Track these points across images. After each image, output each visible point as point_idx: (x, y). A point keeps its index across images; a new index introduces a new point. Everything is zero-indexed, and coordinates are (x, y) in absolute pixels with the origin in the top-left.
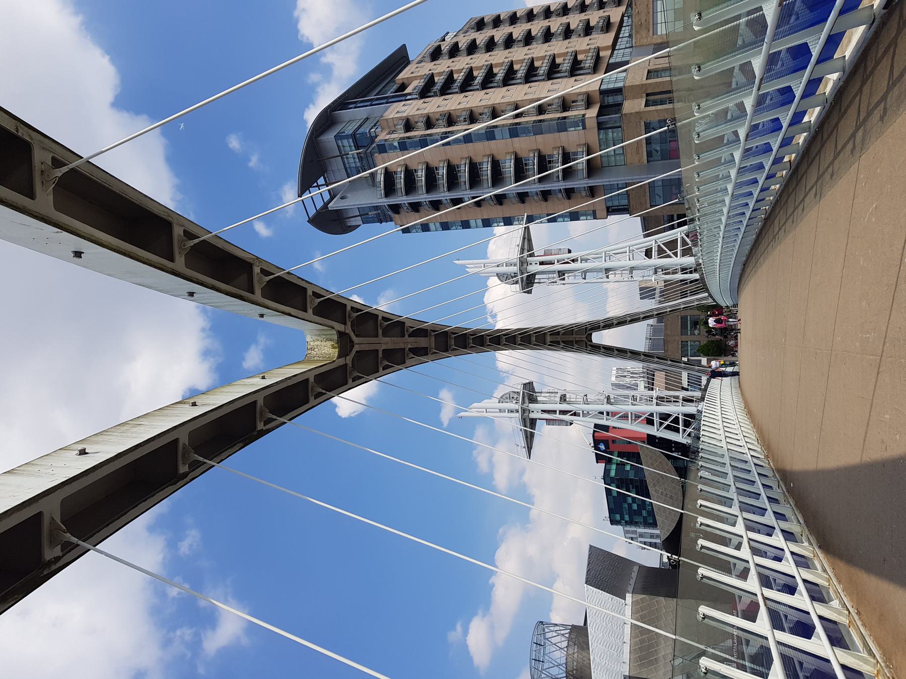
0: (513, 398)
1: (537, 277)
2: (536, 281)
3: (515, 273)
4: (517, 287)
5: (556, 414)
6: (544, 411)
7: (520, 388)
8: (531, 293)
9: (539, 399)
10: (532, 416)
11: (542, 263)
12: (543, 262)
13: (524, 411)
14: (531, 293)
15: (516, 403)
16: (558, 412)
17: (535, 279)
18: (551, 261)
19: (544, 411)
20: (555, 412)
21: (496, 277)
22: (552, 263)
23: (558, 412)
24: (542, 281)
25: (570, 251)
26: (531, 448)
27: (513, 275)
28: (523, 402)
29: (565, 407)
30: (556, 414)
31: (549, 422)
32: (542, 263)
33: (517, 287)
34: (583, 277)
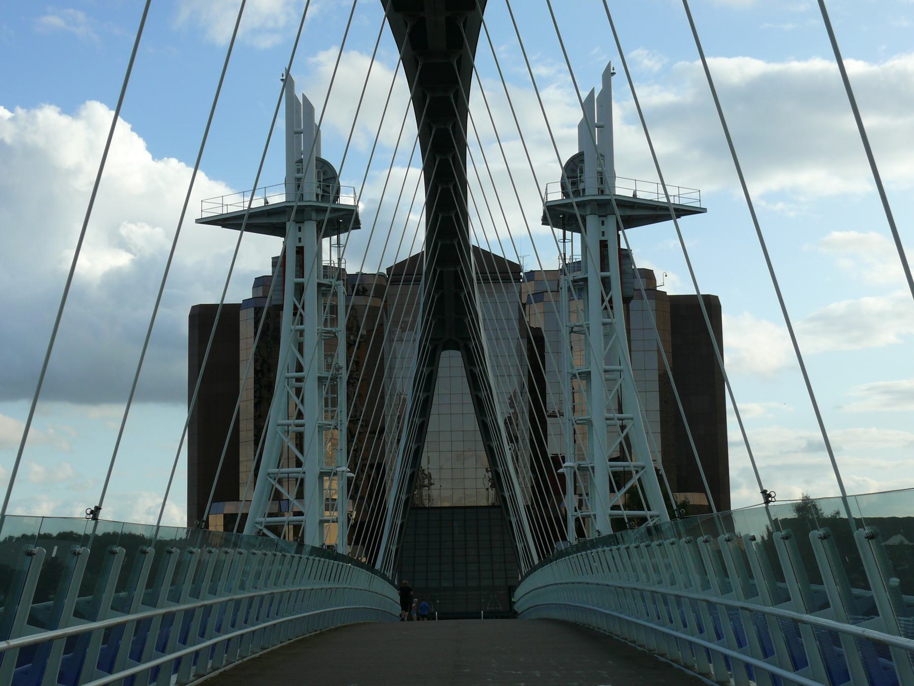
0: (328, 186)
1: (577, 236)
2: (568, 233)
3: (584, 190)
4: (556, 195)
5: (297, 277)
6: (300, 251)
7: (346, 199)
8: (543, 224)
9: (326, 242)
10: (291, 227)
11: (604, 245)
12: (606, 246)
13: (301, 210)
14: (543, 224)
15: (317, 195)
16: (300, 280)
17: (573, 231)
18: (608, 265)
19: (300, 251)
21: (575, 151)
22: (604, 266)
23: (300, 280)
24: (568, 245)
26: (224, 226)
27: (581, 186)
29: (311, 294)
30: (297, 277)
31: (279, 263)
32: (604, 245)
33: (556, 195)
34: (575, 329)
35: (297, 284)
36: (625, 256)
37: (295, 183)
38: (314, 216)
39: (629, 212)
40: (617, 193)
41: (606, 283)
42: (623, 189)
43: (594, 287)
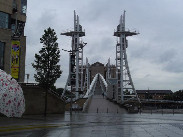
6: (76, 39)
10: (75, 35)
11: (123, 39)
13: (76, 32)
19: (76, 39)
20: (76, 42)
22: (123, 42)
25: (127, 48)
28: (79, 32)
31: (73, 41)
32: (123, 39)
33: (116, 31)
35: (75, 44)
36: (126, 41)
37: (76, 28)
38: (78, 33)
39: (127, 34)
40: (126, 30)
41: (123, 45)
42: (127, 30)
43: (122, 45)
